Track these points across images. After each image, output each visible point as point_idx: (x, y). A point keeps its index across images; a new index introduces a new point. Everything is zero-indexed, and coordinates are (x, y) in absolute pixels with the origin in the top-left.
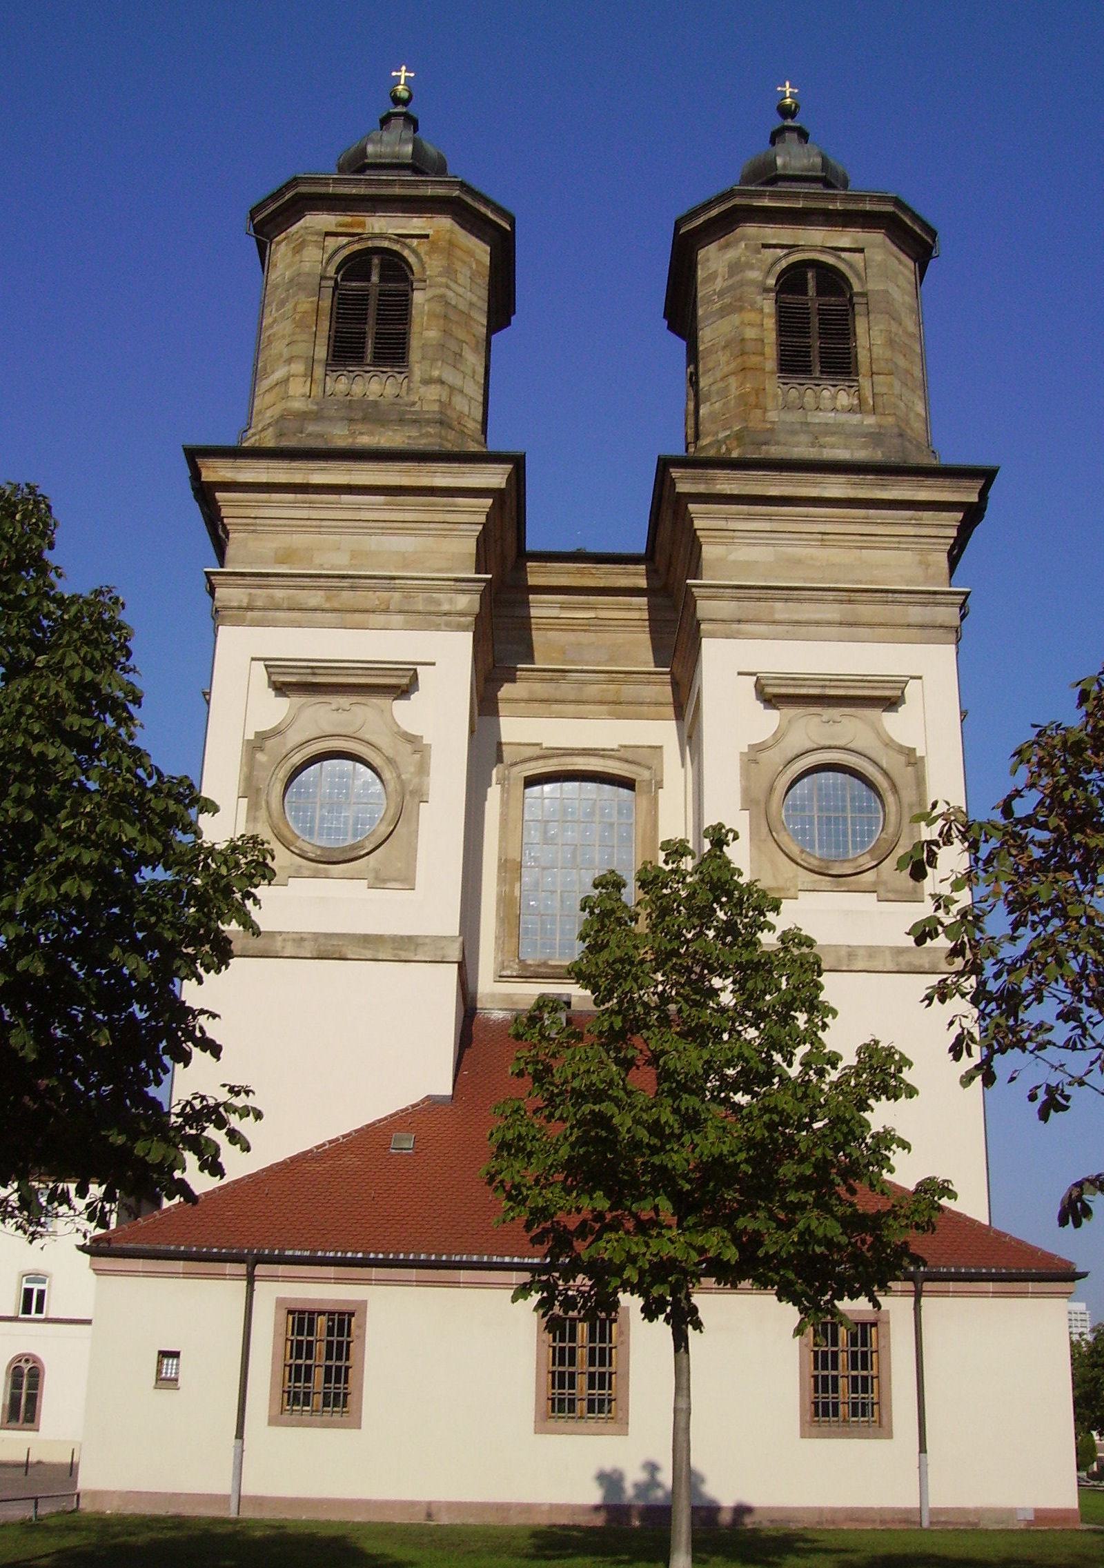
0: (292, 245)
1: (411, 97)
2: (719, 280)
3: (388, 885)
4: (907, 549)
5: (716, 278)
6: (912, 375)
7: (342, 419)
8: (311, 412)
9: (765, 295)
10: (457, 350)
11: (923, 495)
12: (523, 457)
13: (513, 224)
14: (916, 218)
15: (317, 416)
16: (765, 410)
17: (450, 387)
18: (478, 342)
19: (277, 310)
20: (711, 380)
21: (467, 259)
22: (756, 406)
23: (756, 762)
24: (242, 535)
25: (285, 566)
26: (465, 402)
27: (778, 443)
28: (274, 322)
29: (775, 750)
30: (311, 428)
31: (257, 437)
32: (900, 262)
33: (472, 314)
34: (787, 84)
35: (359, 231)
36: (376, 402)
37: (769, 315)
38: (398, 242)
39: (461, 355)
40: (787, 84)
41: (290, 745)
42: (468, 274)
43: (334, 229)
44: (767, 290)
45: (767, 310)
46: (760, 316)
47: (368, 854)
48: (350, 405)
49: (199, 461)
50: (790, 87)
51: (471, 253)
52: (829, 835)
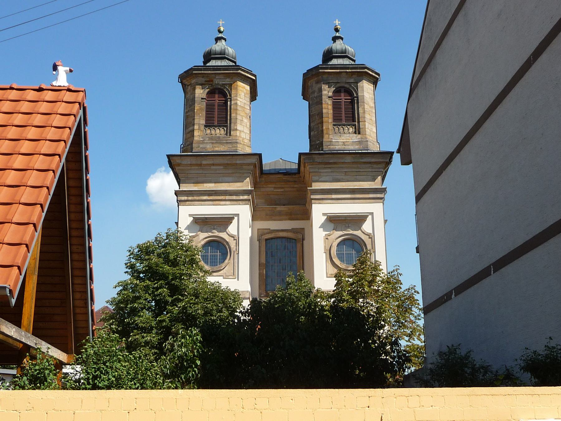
0: (192, 88)
1: (223, 32)
2: (316, 93)
3: (229, 277)
4: (370, 175)
5: (315, 92)
6: (372, 120)
7: (210, 143)
8: (201, 141)
9: (329, 99)
10: (242, 119)
11: (373, 160)
12: (261, 154)
13: (256, 78)
14: (373, 71)
15: (203, 142)
16: (329, 134)
17: (240, 131)
18: (247, 115)
19: (189, 108)
20: (314, 124)
21: (242, 90)
22: (327, 134)
23: (327, 239)
24: (184, 178)
25: (196, 187)
26: (244, 134)
27: (333, 145)
28: (189, 111)
29: (333, 235)
30: (201, 146)
31: (186, 148)
32: (368, 84)
33: (245, 107)
34: (337, 20)
35: (211, 83)
36: (219, 137)
37: (330, 105)
38: (222, 86)
39: (242, 120)
40: (337, 20)
41: (201, 239)
42: (243, 94)
43: (204, 83)
44: (329, 97)
45: (329, 103)
46: (327, 106)
47: (224, 269)
48: (211, 139)
49: (171, 158)
50: (338, 21)
51: (244, 88)
52: (348, 258)
